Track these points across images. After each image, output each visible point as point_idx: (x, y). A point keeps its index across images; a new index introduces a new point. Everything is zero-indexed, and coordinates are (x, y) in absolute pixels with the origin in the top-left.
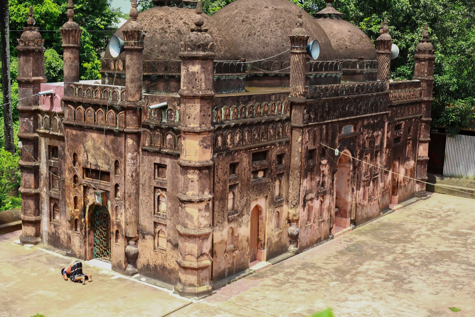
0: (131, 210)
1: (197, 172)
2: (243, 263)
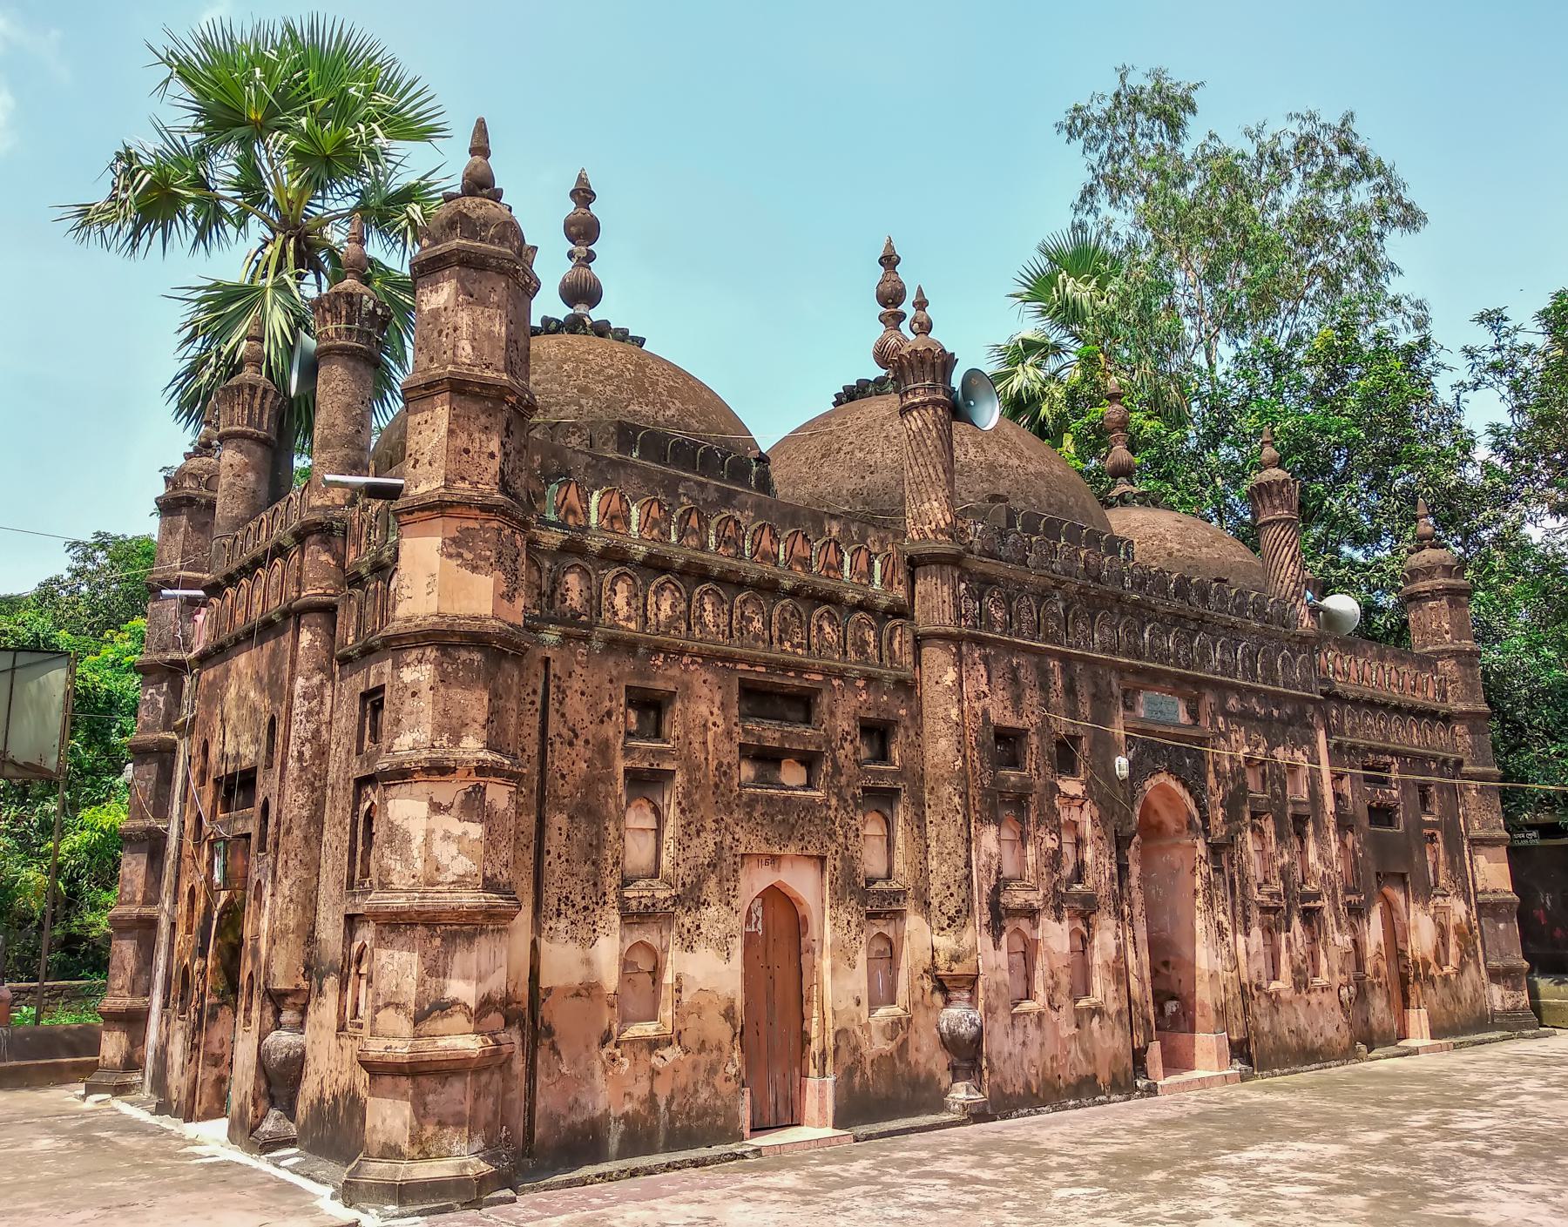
1: (431, 653)
2: (704, 1112)
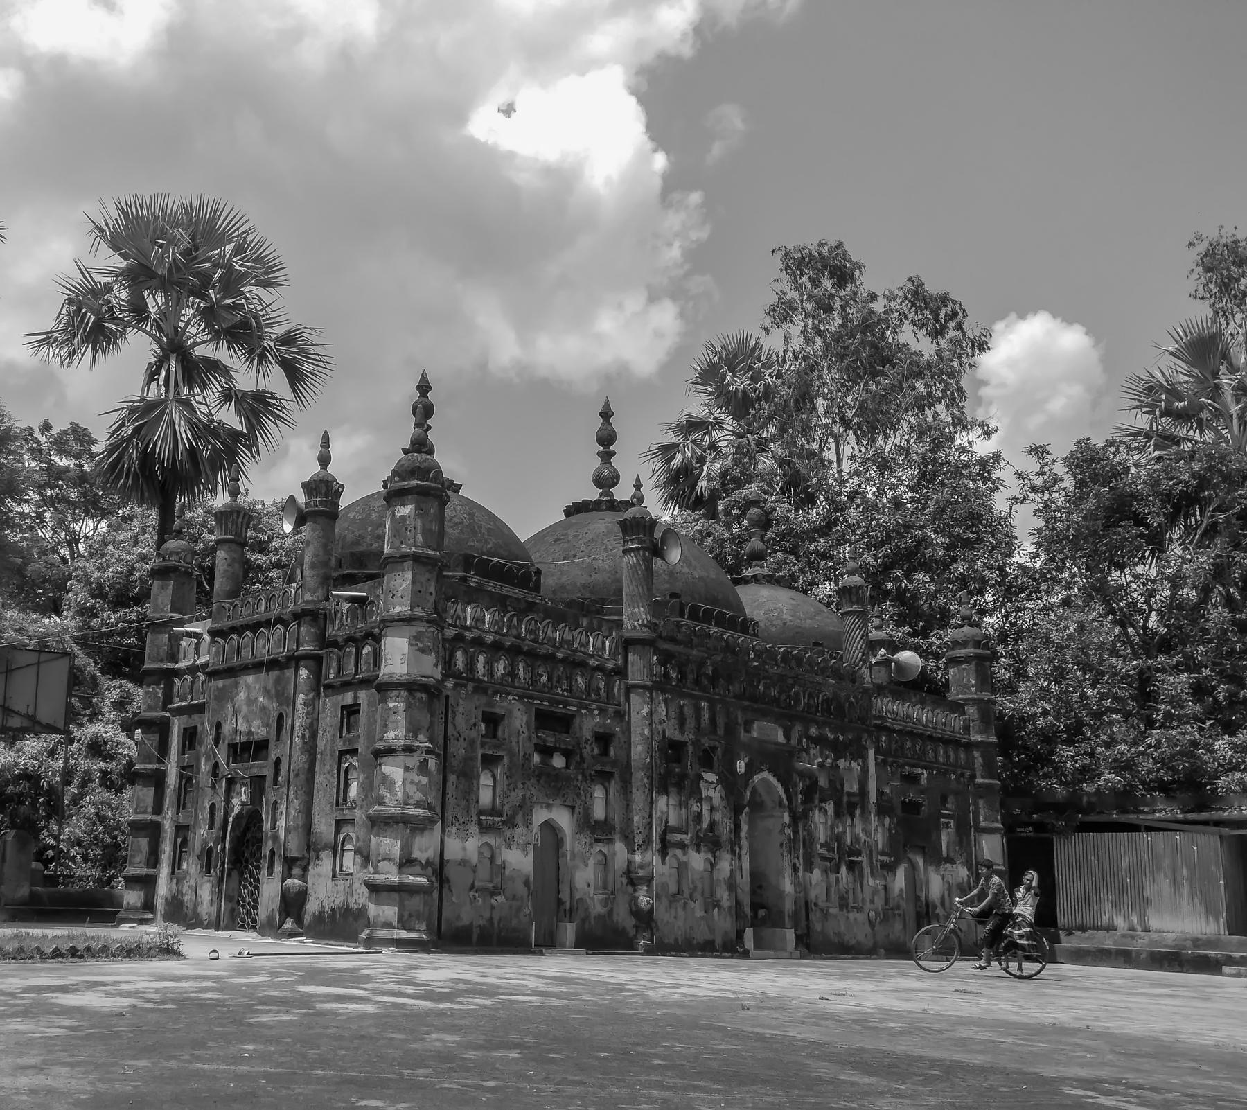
0: (297, 802)
1: (404, 693)
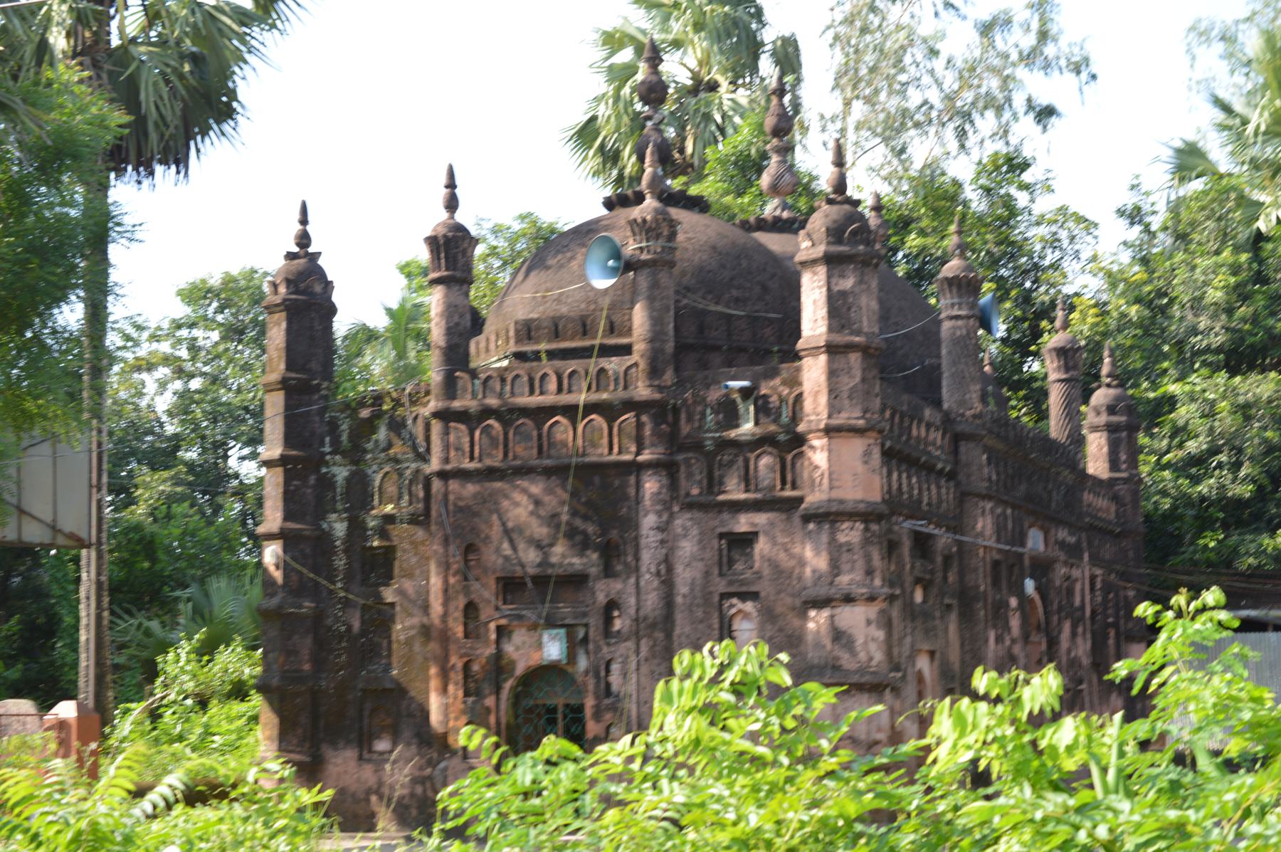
1: (860, 526)
